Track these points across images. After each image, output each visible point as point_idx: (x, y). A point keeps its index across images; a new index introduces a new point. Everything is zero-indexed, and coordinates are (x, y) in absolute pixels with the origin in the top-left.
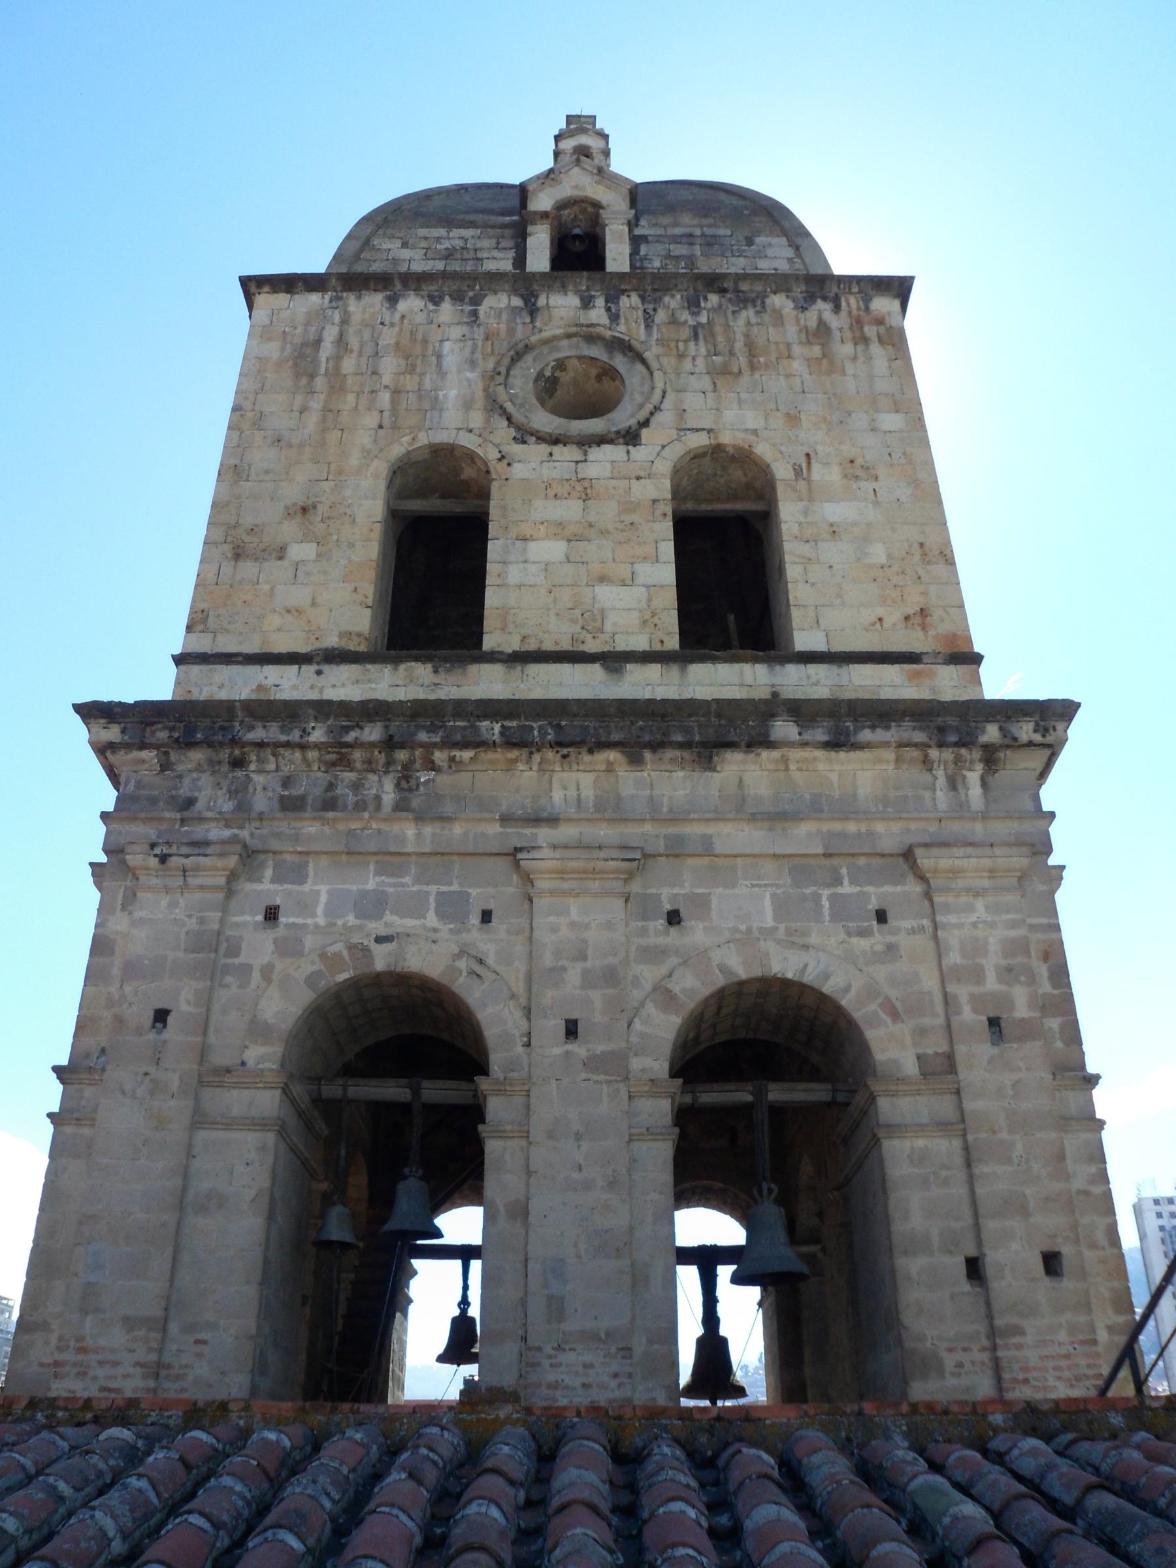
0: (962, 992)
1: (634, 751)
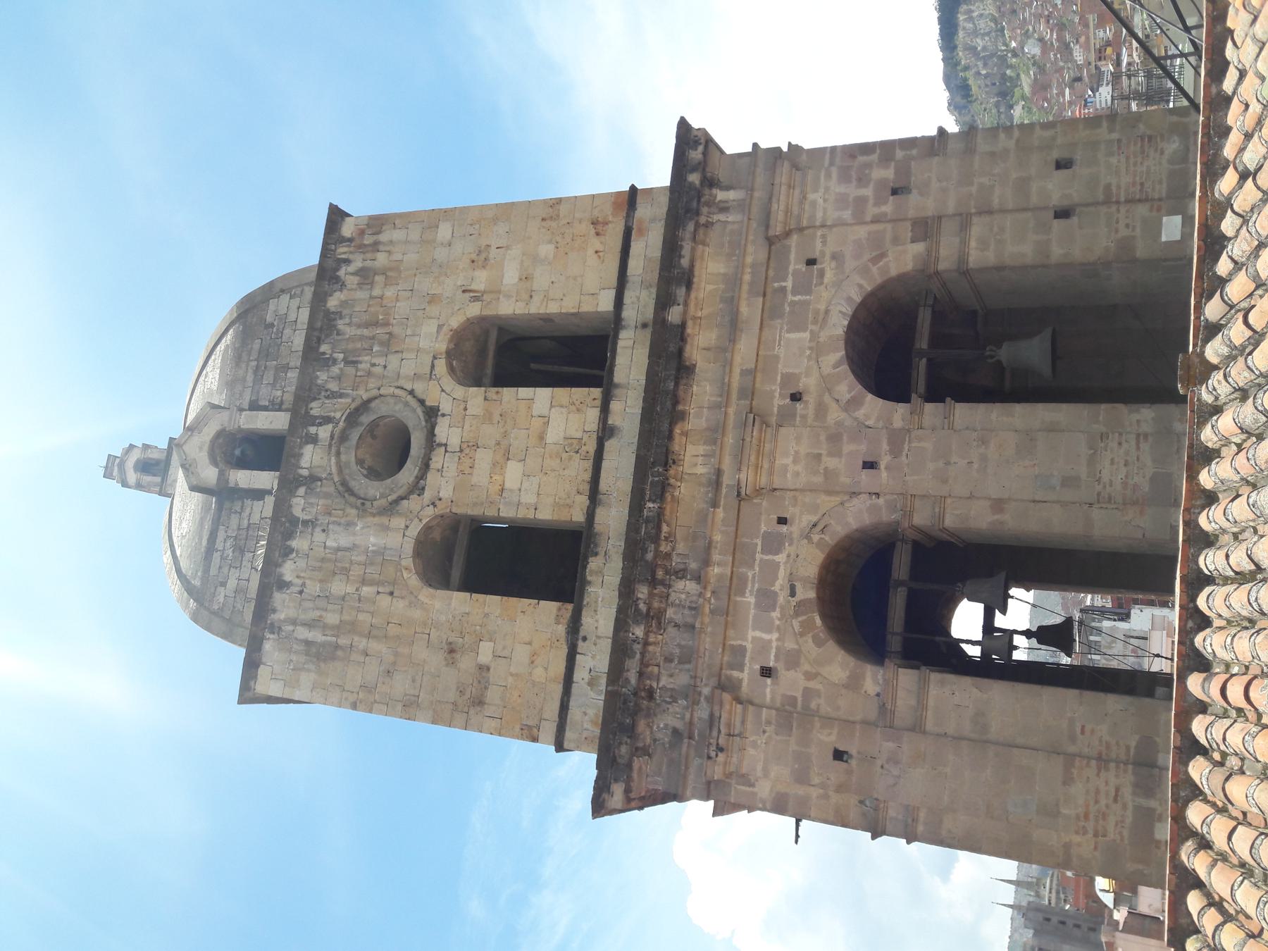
0: (872, 211)
1: (677, 416)
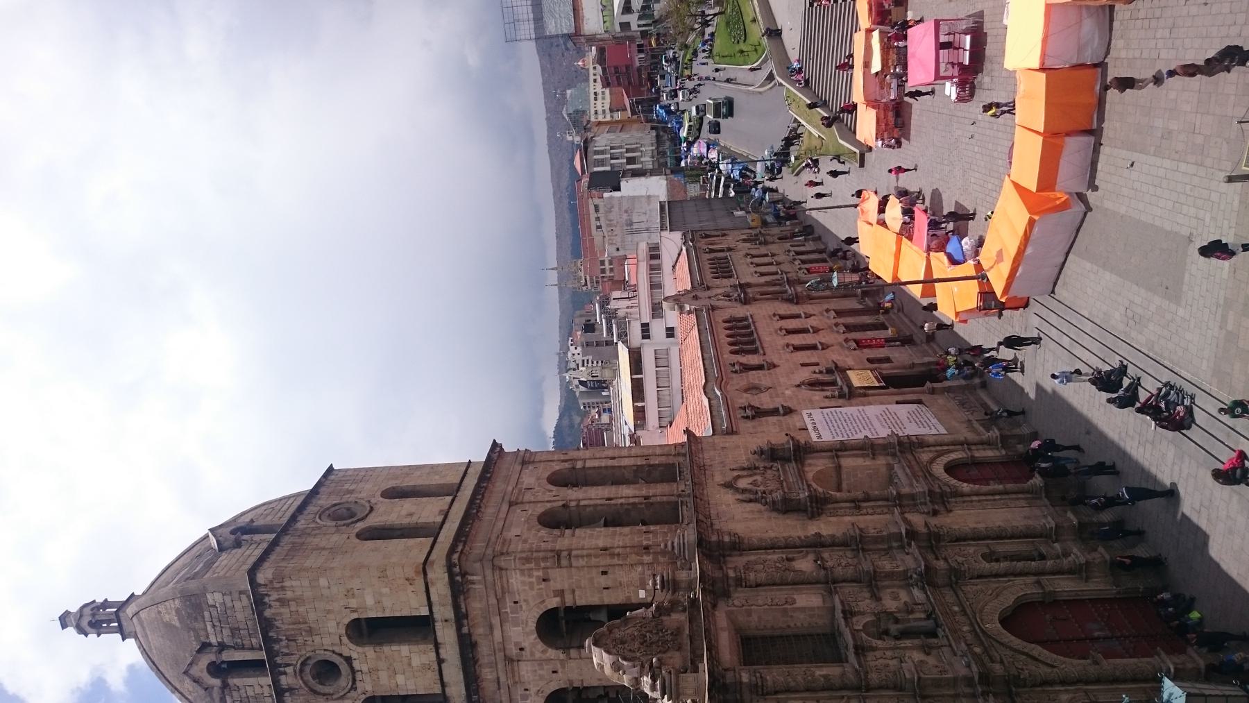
1: (475, 661)
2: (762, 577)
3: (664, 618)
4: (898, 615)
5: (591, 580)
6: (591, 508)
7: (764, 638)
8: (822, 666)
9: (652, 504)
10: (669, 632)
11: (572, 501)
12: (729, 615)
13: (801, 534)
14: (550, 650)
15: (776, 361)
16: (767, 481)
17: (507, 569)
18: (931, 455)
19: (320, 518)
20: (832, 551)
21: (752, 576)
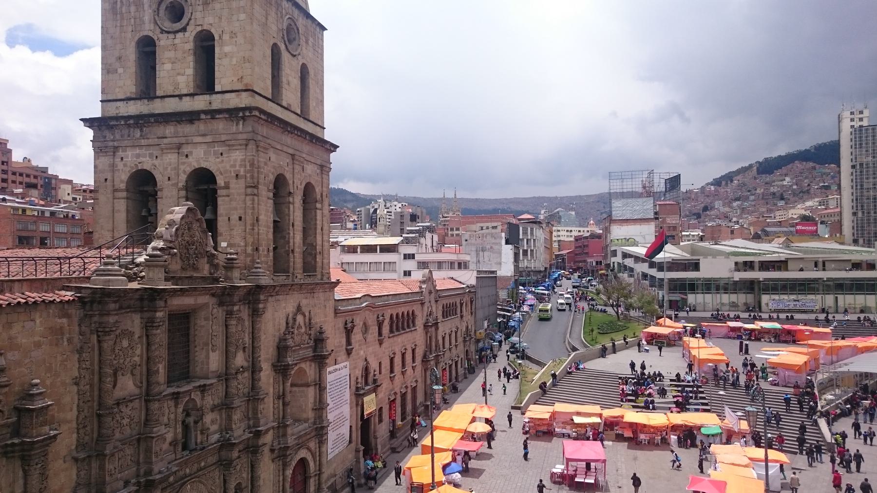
2: (233, 329)
3: (206, 259)
4: (200, 424)
5: (236, 209)
6: (287, 212)
7: (188, 329)
8: (165, 369)
9: (288, 255)
10: (195, 262)
11: (293, 199)
12: (206, 305)
13: (262, 358)
14: (186, 176)
15: (384, 345)
16: (300, 336)
17: (246, 149)
18: (313, 449)
19: (289, 18)
20: (249, 379)
21: (234, 322)
